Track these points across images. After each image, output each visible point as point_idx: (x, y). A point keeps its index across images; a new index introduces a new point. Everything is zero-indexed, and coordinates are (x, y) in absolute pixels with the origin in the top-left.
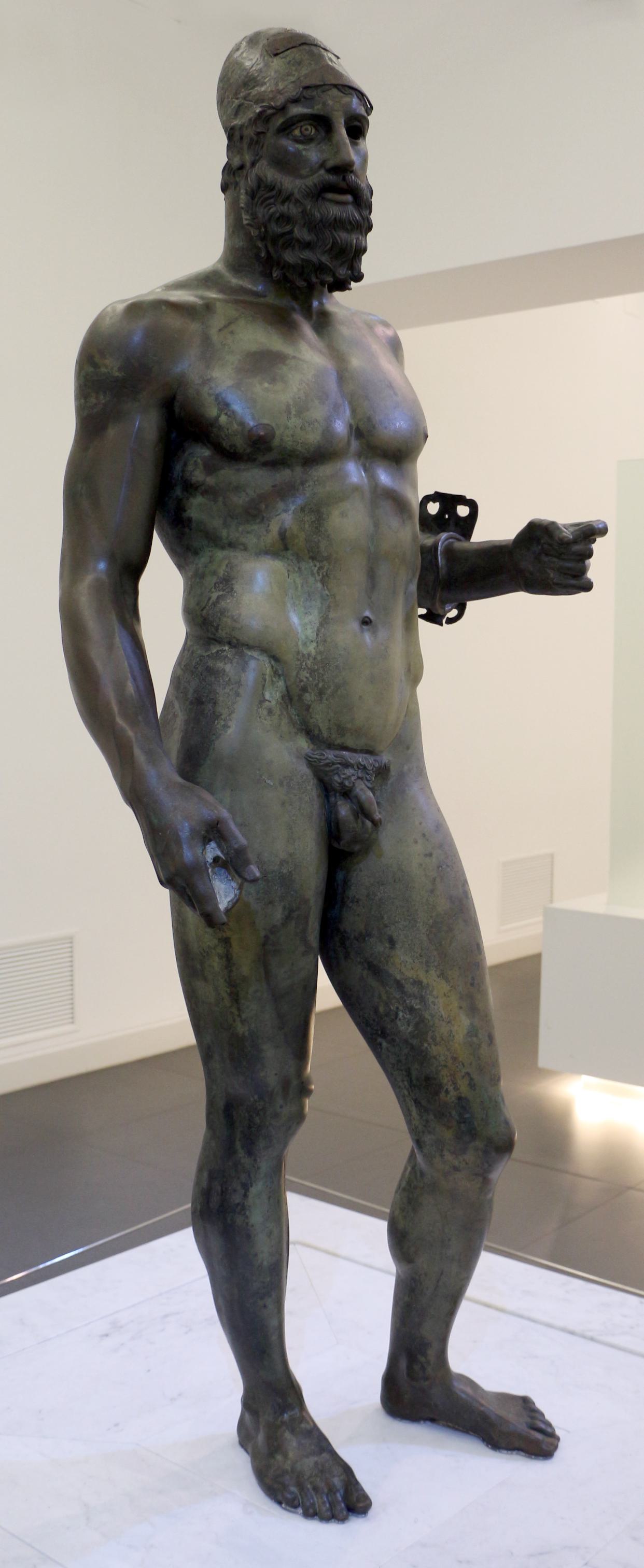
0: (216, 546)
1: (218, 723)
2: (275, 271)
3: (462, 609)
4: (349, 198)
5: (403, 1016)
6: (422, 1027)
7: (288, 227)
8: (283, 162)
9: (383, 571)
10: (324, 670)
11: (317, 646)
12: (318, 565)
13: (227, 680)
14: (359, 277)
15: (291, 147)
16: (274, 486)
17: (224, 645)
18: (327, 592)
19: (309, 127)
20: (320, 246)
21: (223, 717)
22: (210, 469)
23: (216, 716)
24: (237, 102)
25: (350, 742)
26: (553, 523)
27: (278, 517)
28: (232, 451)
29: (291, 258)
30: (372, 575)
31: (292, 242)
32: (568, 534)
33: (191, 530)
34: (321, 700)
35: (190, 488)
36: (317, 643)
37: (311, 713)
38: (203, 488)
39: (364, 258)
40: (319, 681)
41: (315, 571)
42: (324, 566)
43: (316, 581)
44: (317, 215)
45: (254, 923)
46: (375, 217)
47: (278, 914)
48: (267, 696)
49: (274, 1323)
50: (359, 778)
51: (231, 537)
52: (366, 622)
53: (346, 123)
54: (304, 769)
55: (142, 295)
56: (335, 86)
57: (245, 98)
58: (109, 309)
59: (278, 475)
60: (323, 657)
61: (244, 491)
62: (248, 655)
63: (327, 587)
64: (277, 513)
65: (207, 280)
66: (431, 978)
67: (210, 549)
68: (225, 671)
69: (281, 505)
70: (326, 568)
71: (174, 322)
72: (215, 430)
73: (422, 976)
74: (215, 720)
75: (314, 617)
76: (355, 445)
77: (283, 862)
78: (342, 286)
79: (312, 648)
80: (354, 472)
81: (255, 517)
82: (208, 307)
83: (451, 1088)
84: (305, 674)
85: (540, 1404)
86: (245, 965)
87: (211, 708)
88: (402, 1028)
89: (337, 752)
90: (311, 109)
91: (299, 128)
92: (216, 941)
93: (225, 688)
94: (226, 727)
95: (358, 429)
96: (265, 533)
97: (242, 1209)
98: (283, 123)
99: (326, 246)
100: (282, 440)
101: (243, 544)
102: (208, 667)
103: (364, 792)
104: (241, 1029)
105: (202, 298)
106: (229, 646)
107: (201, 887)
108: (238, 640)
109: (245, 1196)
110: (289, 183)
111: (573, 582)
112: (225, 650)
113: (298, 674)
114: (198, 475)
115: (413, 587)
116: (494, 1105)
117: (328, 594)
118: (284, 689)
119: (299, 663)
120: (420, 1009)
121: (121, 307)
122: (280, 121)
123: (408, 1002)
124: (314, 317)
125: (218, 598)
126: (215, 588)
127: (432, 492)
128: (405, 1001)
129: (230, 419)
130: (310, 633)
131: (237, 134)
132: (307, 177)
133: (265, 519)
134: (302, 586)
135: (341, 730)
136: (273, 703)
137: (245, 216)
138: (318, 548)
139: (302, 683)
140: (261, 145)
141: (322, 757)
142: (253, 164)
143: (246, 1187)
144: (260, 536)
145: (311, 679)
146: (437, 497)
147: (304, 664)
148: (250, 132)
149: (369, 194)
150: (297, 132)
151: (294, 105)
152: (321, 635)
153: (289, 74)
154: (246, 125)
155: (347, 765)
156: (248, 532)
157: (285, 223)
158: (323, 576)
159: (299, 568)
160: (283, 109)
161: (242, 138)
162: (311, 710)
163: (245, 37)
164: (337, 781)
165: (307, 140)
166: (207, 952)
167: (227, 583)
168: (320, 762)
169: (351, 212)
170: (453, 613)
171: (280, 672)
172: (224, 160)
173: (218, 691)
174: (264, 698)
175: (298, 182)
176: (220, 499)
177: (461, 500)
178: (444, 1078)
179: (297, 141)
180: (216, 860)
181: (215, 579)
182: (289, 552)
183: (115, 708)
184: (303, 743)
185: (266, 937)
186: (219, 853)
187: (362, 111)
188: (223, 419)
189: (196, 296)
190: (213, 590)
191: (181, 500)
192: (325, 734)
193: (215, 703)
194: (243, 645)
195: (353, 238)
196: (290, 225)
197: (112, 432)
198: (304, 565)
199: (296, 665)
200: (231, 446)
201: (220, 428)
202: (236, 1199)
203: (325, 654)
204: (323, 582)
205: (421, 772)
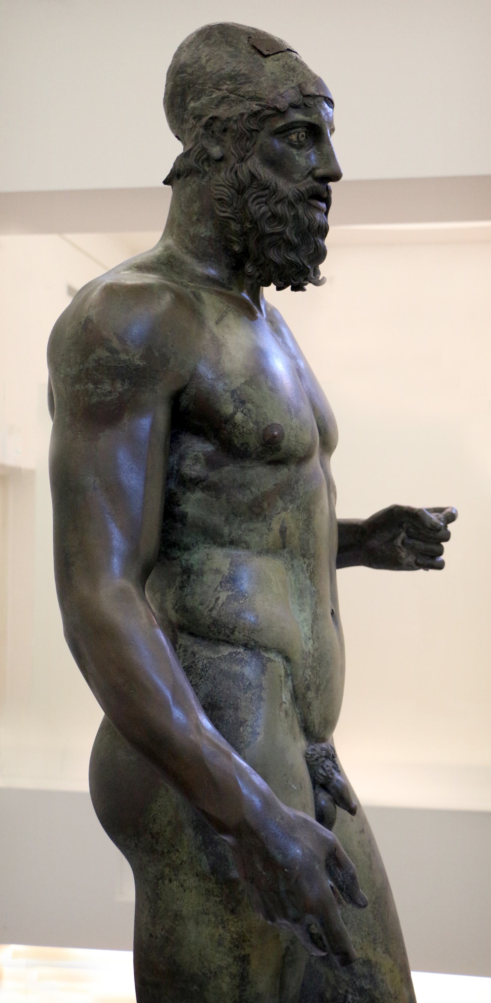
0: (215, 543)
1: (244, 731)
2: (249, 267)
5: (353, 999)
10: (319, 667)
11: (314, 643)
12: (307, 562)
13: (247, 683)
16: (275, 485)
17: (239, 648)
18: (314, 588)
20: (303, 250)
21: (248, 723)
27: (278, 515)
28: (242, 449)
29: (276, 258)
31: (278, 242)
33: (184, 525)
34: (317, 697)
36: (313, 640)
37: (310, 710)
38: (205, 483)
40: (317, 678)
41: (305, 569)
42: (311, 562)
43: (306, 578)
45: (278, 936)
51: (234, 535)
59: (278, 474)
60: (319, 654)
61: (249, 489)
62: (265, 657)
63: (314, 584)
64: (278, 512)
67: (206, 545)
68: (243, 675)
70: (312, 566)
72: (229, 427)
73: (371, 956)
74: (240, 726)
81: (258, 515)
87: (231, 713)
90: (310, 117)
91: (297, 134)
92: (231, 960)
93: (246, 692)
96: (267, 531)
98: (284, 125)
99: (309, 251)
100: (288, 440)
101: (245, 542)
102: (221, 670)
106: (244, 648)
108: (255, 642)
111: (429, 562)
112: (240, 652)
113: (303, 673)
117: (315, 591)
118: (292, 688)
119: (304, 661)
120: (370, 989)
123: (357, 983)
125: (228, 598)
126: (221, 588)
128: (355, 982)
129: (245, 417)
132: (298, 181)
133: (267, 517)
134: (295, 583)
136: (288, 703)
138: (308, 546)
139: (307, 682)
140: (253, 141)
141: (314, 752)
144: (263, 535)
145: (312, 677)
147: (307, 663)
150: (294, 137)
151: (295, 110)
152: (315, 632)
154: (235, 118)
156: (251, 530)
157: (276, 224)
158: (311, 572)
162: (311, 708)
164: (322, 775)
166: (215, 972)
168: (312, 757)
171: (289, 672)
173: (238, 696)
174: (282, 700)
175: (291, 186)
176: (224, 496)
181: (219, 578)
182: (286, 550)
185: (288, 948)
188: (239, 417)
190: (219, 589)
191: (175, 494)
193: (236, 709)
194: (261, 647)
196: (282, 226)
198: (296, 562)
199: (303, 664)
200: (242, 444)
201: (235, 425)
203: (319, 650)
204: (311, 580)
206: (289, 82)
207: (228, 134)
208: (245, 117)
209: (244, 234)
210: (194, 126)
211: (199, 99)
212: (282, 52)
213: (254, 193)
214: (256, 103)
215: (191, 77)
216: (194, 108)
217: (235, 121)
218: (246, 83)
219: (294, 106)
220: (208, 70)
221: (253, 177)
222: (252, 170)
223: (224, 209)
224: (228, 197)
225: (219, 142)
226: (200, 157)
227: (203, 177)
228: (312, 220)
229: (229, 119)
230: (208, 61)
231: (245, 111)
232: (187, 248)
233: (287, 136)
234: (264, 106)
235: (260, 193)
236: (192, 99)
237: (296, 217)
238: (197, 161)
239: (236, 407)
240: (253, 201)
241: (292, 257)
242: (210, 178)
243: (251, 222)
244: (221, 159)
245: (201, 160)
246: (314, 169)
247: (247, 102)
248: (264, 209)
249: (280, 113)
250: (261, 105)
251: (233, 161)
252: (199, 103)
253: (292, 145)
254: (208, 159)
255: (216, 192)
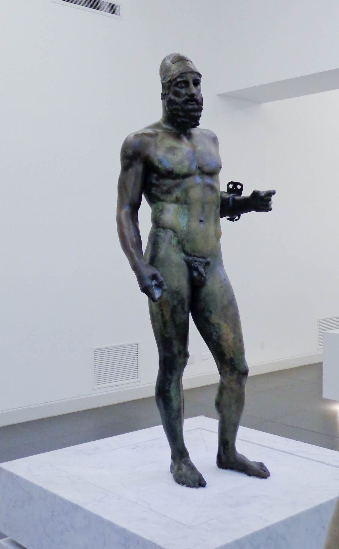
3: (239, 216)
4: (194, 103)
6: (219, 337)
8: (177, 94)
9: (207, 207)
14: (198, 124)
15: (177, 89)
19: (182, 84)
22: (157, 179)
23: (158, 248)
24: (164, 76)
25: (197, 254)
26: (259, 191)
30: (203, 208)
32: (263, 194)
35: (153, 185)
39: (200, 118)
44: (186, 108)
46: (203, 107)
47: (176, 302)
48: (172, 242)
49: (179, 429)
50: (199, 265)
52: (201, 221)
53: (193, 82)
54: (184, 263)
55: (137, 132)
56: (190, 72)
57: (166, 75)
58: (129, 136)
65: (157, 126)
66: (222, 323)
69: (176, 189)
71: (147, 139)
75: (186, 220)
76: (198, 172)
77: (177, 288)
78: (194, 126)
79: (185, 229)
80: (198, 179)
82: (156, 134)
83: (228, 355)
84: (183, 236)
85: (265, 464)
86: (167, 317)
88: (214, 337)
89: (192, 258)
94: (161, 250)
95: (199, 167)
97: (168, 391)
103: (201, 269)
104: (167, 336)
105: (155, 131)
107: (151, 291)
109: (169, 387)
110: (177, 99)
111: (266, 208)
114: (154, 181)
115: (218, 210)
116: (243, 360)
121: (132, 136)
122: (174, 83)
124: (187, 135)
127: (230, 182)
130: (185, 224)
131: (164, 85)
135: (194, 251)
137: (167, 108)
142: (168, 94)
143: (170, 384)
146: (232, 183)
148: (167, 85)
149: (201, 100)
150: (179, 86)
153: (177, 69)
155: (196, 261)
159: (182, 207)
160: (175, 79)
161: (165, 86)
163: (166, 56)
165: (182, 88)
167: (162, 211)
169: (196, 106)
170: (237, 218)
172: (161, 92)
175: (180, 100)
177: (239, 184)
178: (226, 351)
179: (180, 88)
180: (156, 285)
183: (130, 245)
184: (183, 255)
186: (157, 283)
187: (199, 78)
188: (160, 166)
189: (153, 131)
192: (189, 252)
195: (196, 114)
197: (130, 170)
202: (167, 388)
204: (188, 210)
205: (221, 264)
239: (159, 164)
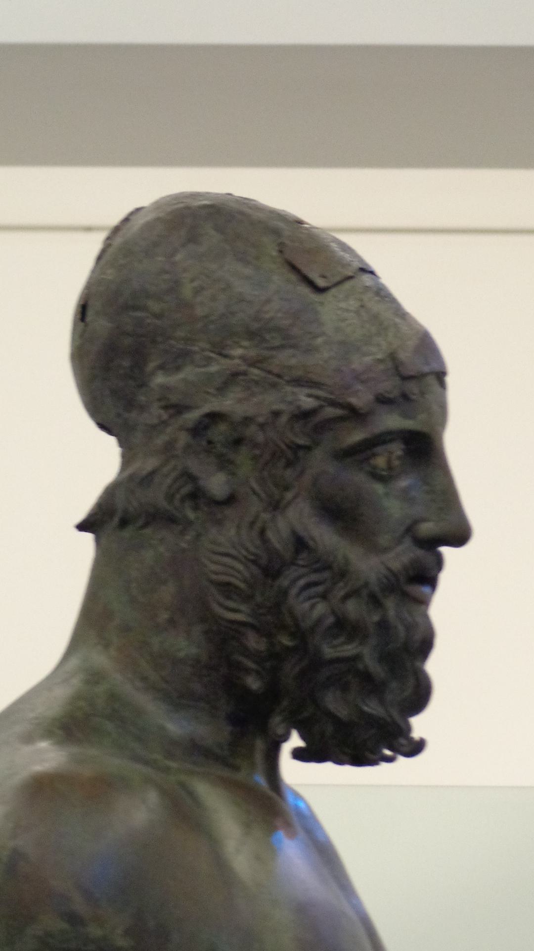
7: (350, 647)
132: (386, 550)
150: (380, 462)
154: (261, 420)
157: (342, 639)
206: (374, 349)
207: (244, 450)
208: (284, 419)
209: (276, 656)
210: (164, 423)
211: (178, 369)
212: (350, 278)
213: (299, 578)
214: (307, 391)
215: (158, 322)
216: (166, 388)
217: (262, 426)
218: (282, 347)
219: (383, 400)
220: (199, 311)
221: (300, 544)
222: (299, 529)
223: (231, 604)
224: (245, 581)
225: (224, 464)
226: (178, 490)
227: (182, 533)
228: (410, 628)
229: (247, 420)
230: (197, 291)
231: (282, 407)
232: (144, 679)
233: (367, 459)
234: (325, 399)
235: (314, 577)
236: (161, 367)
237: (384, 626)
238: (170, 497)
240: (299, 594)
241: (372, 707)
242: (198, 536)
243: (293, 635)
244: (231, 500)
245: (178, 496)
246: (416, 522)
247: (289, 389)
248: (321, 608)
249: (355, 415)
250: (317, 398)
251: (255, 506)
252: (181, 376)
253: (376, 476)
254: (197, 496)
255: (214, 567)
